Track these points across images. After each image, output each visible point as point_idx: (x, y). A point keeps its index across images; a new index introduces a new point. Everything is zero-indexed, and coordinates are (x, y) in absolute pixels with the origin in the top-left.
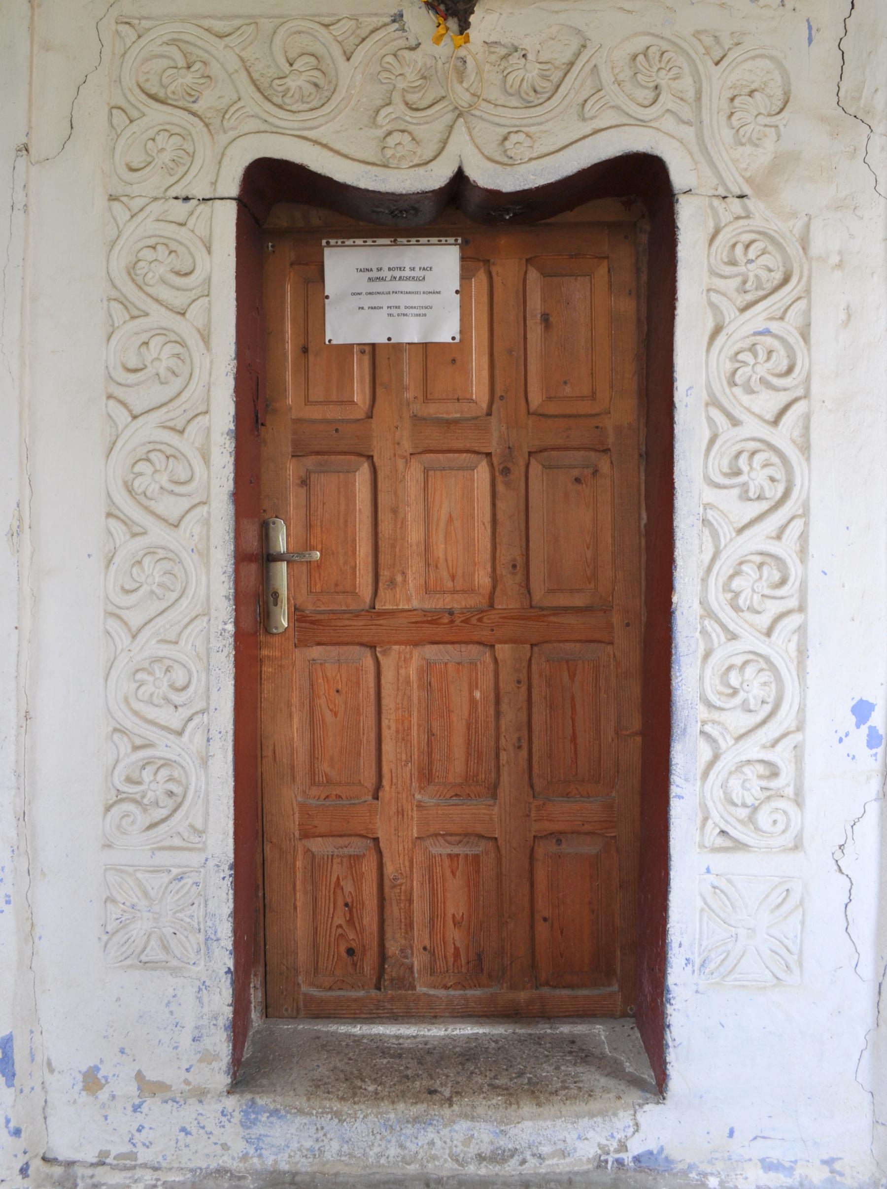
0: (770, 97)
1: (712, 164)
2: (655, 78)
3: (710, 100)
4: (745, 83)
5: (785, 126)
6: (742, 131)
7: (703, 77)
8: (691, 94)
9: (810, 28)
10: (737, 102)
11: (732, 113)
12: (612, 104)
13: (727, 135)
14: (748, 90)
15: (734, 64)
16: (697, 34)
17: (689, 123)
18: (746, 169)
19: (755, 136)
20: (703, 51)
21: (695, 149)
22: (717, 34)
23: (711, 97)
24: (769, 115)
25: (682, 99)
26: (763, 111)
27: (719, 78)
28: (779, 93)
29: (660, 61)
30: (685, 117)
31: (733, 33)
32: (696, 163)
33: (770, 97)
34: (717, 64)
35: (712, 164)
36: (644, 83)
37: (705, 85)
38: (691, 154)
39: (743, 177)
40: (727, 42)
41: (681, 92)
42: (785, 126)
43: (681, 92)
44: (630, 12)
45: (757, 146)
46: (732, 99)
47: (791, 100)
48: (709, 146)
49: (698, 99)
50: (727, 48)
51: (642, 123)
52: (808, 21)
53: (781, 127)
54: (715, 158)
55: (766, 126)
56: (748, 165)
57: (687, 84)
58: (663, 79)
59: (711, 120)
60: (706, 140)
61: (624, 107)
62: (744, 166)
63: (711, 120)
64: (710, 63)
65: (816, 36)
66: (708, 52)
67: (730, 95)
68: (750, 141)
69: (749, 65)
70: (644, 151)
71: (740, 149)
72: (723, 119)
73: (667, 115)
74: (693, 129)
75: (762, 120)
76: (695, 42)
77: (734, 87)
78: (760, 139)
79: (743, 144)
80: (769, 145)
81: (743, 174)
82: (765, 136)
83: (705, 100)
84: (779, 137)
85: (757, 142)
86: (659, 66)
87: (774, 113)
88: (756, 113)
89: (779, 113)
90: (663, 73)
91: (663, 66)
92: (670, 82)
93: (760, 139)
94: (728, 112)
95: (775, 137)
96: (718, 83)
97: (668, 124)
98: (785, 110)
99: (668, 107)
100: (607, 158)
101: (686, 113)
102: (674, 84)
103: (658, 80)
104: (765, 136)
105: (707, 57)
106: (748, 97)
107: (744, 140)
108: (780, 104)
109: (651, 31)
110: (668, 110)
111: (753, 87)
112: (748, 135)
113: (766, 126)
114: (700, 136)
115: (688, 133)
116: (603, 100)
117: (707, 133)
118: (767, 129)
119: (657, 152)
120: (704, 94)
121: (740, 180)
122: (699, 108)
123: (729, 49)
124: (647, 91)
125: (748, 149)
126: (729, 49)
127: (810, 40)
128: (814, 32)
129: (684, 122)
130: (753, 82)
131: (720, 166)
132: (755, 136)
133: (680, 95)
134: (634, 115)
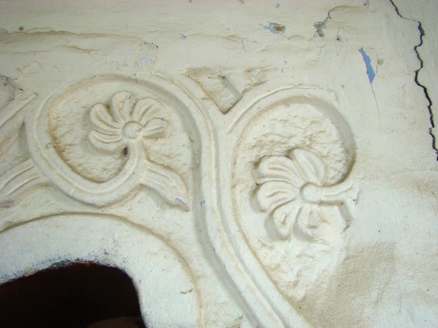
0: (322, 157)
1: (224, 276)
2: (121, 137)
3: (217, 166)
4: (277, 139)
5: (356, 201)
6: (279, 216)
7: (203, 132)
8: (185, 158)
9: (367, 59)
10: (264, 167)
11: (258, 186)
12: (43, 179)
13: (254, 223)
14: (284, 148)
15: (254, 111)
16: (194, 73)
17: (180, 206)
18: (295, 284)
19: (304, 222)
20: (203, 95)
21: (194, 251)
22: (225, 73)
23: (217, 161)
24: (325, 185)
25: (168, 168)
26: (313, 179)
27: (231, 131)
28: (337, 150)
29: (131, 113)
30: (171, 196)
31: (249, 71)
32: (194, 278)
33: (322, 157)
34: (225, 112)
35: (224, 276)
36: (99, 145)
37: (207, 143)
38: (184, 261)
39: (290, 300)
40: (240, 82)
41: (168, 156)
42: (356, 201)
43: (168, 156)
44: (88, 51)
45: (310, 239)
46: (256, 164)
47: (358, 159)
48: (217, 245)
49: (196, 166)
50: (240, 89)
51: (96, 210)
52: (361, 51)
53: (350, 203)
54: (230, 269)
55: (321, 203)
56: (298, 275)
57: (178, 144)
58: (135, 138)
59: (219, 198)
60: (211, 234)
61: (62, 184)
62: (290, 277)
63: (219, 198)
64: (213, 110)
65: (379, 71)
66: (210, 96)
67: (252, 156)
68: (296, 229)
69: (281, 112)
70: (92, 259)
71: (280, 247)
72: (242, 196)
73: (143, 194)
74: (189, 216)
75: (312, 193)
76: (190, 84)
77: (260, 145)
78: (314, 227)
79: (284, 239)
80: (332, 233)
81: (290, 293)
82: (324, 221)
83: (208, 165)
84: (348, 221)
85: (309, 232)
86: (128, 119)
87: (333, 182)
88: (301, 183)
89: (341, 181)
90: (132, 129)
91: (136, 119)
92: (148, 143)
93: (314, 227)
94: (252, 183)
95: (340, 222)
96: (229, 143)
97: (144, 209)
98: (352, 175)
99: (142, 181)
100: (20, 275)
101: (175, 189)
102: (156, 146)
103: (126, 140)
104: (324, 221)
105: (208, 103)
106: (284, 159)
107: (284, 231)
108: (341, 167)
109: (118, 72)
110: (142, 187)
111: (292, 143)
112: (290, 222)
113: (321, 203)
114: (201, 227)
115: (181, 224)
116: (27, 173)
117: (213, 222)
118: (325, 209)
119: (116, 261)
120: (204, 155)
121: (285, 308)
122: (198, 180)
123: (245, 91)
124: (108, 159)
125: (296, 246)
126: (245, 91)
127: (371, 75)
128: (373, 64)
129: (172, 206)
130: (290, 137)
131: (242, 282)
132: (304, 222)
133: (167, 161)
134: (77, 195)
